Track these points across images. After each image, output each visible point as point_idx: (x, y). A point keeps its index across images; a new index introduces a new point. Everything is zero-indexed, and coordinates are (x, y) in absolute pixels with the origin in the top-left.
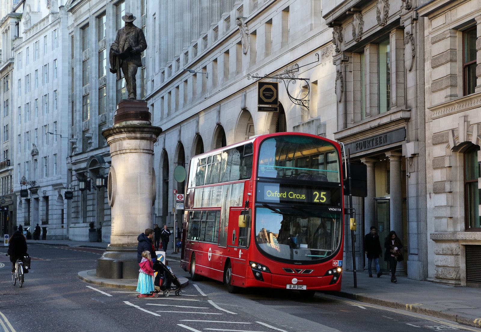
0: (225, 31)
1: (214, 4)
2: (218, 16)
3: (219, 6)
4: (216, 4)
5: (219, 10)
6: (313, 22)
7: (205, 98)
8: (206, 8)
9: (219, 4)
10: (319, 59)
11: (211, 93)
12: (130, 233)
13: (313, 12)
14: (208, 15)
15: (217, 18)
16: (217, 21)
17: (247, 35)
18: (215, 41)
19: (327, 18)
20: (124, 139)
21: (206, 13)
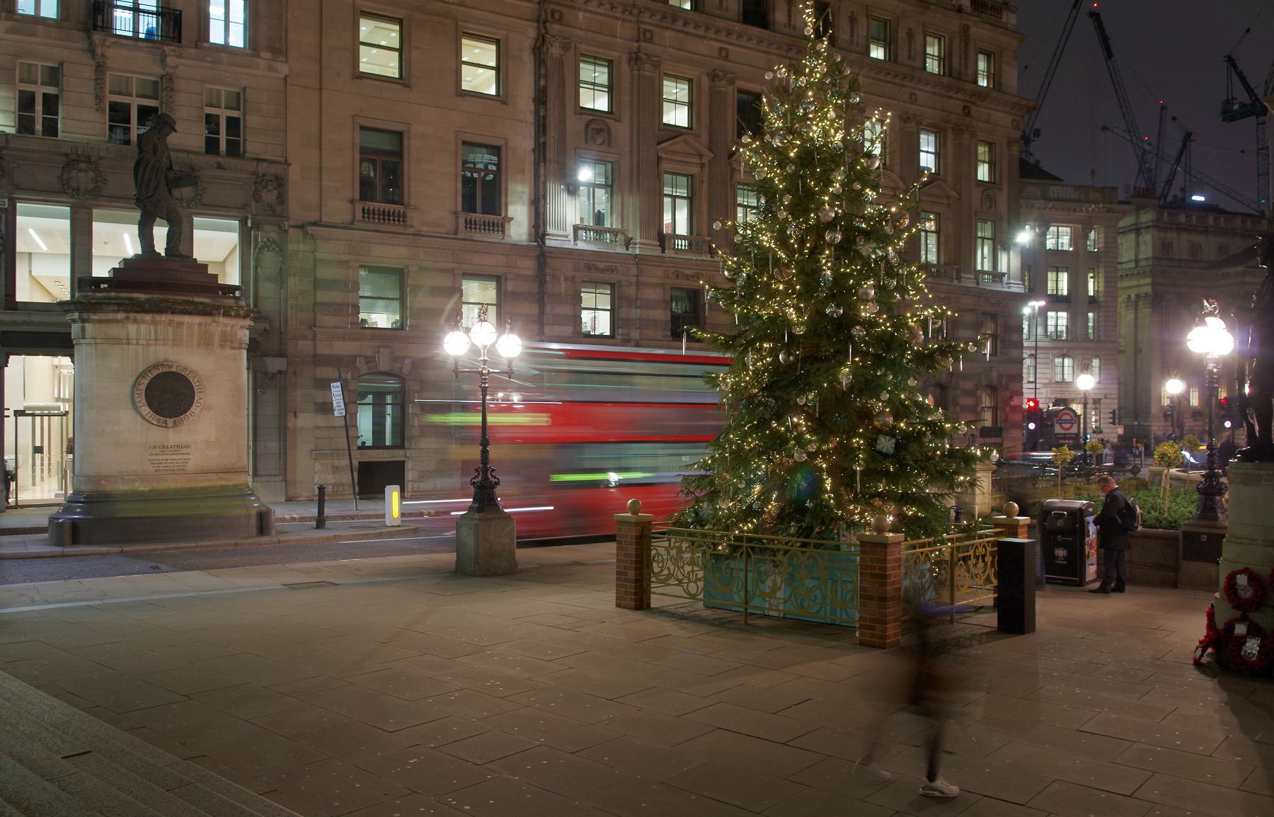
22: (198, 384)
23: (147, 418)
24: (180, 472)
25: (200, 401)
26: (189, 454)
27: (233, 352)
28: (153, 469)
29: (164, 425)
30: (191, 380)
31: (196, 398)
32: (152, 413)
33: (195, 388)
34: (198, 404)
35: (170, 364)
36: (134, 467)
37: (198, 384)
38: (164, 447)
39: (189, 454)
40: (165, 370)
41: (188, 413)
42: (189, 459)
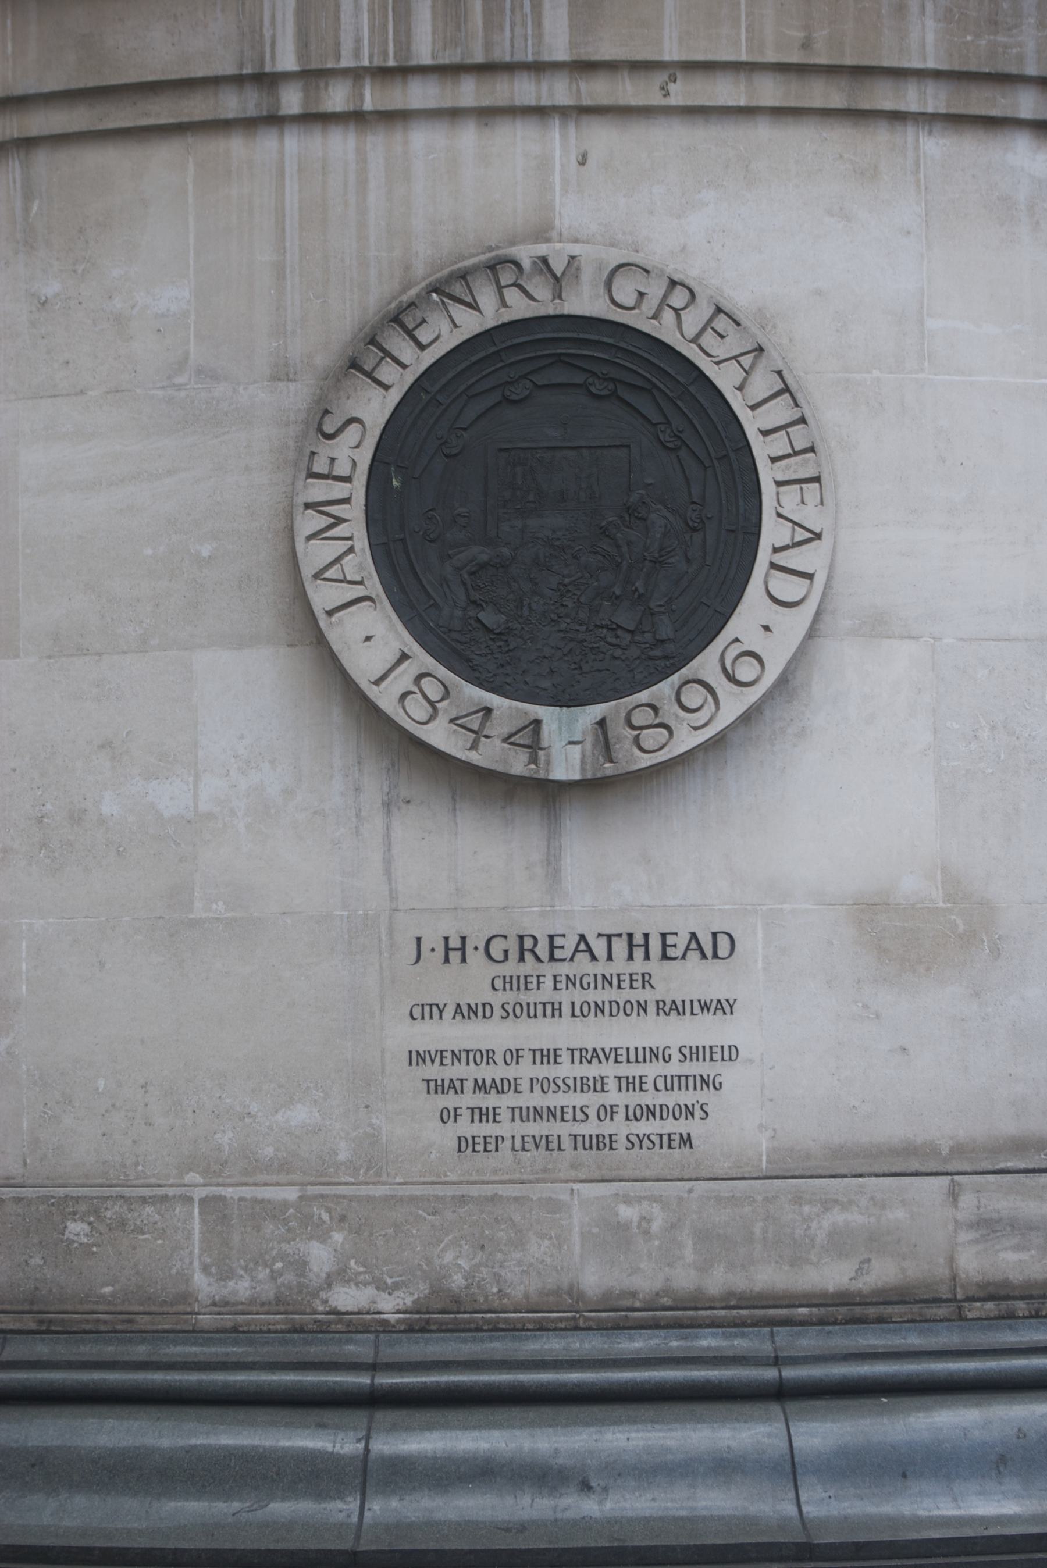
22: (779, 412)
23: (386, 699)
24: (660, 1159)
26: (724, 1007)
28: (445, 1137)
29: (518, 765)
30: (725, 379)
32: (424, 660)
33: (761, 449)
34: (788, 588)
35: (558, 254)
36: (300, 1115)
37: (779, 412)
38: (525, 946)
39: (724, 1007)
40: (519, 308)
42: (731, 1053)
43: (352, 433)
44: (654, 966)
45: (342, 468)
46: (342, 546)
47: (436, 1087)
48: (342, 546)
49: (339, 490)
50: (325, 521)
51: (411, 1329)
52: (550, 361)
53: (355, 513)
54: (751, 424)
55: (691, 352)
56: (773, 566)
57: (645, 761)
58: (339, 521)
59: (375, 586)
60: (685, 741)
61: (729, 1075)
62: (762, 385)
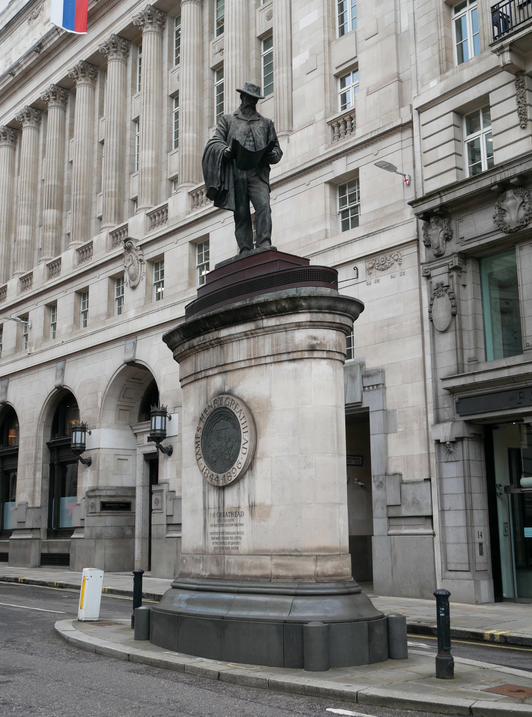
0: (76, 263)
1: (48, 233)
2: (52, 249)
3: (54, 237)
4: (51, 234)
5: (54, 242)
6: (329, 227)
7: (29, 354)
8: (25, 241)
9: (54, 234)
10: (357, 274)
11: (41, 346)
12: (320, 549)
13: (328, 212)
14: (27, 251)
15: (50, 251)
16: (50, 255)
17: (141, 262)
18: (48, 279)
19: (415, 205)
20: (299, 326)
21: (24, 247)
22: (243, 421)
25: (246, 446)
27: (292, 365)
30: (237, 415)
31: (243, 441)
39: (241, 525)
41: (235, 466)
43: (200, 431)
44: (234, 518)
45: (199, 437)
46: (199, 449)
47: (213, 538)
48: (199, 449)
49: (199, 440)
50: (197, 445)
51: (207, 579)
52: (218, 416)
53: (200, 443)
54: (241, 422)
55: (234, 411)
56: (243, 447)
57: (229, 482)
58: (199, 445)
59: (202, 456)
60: (233, 478)
61: (243, 537)
62: (242, 416)
